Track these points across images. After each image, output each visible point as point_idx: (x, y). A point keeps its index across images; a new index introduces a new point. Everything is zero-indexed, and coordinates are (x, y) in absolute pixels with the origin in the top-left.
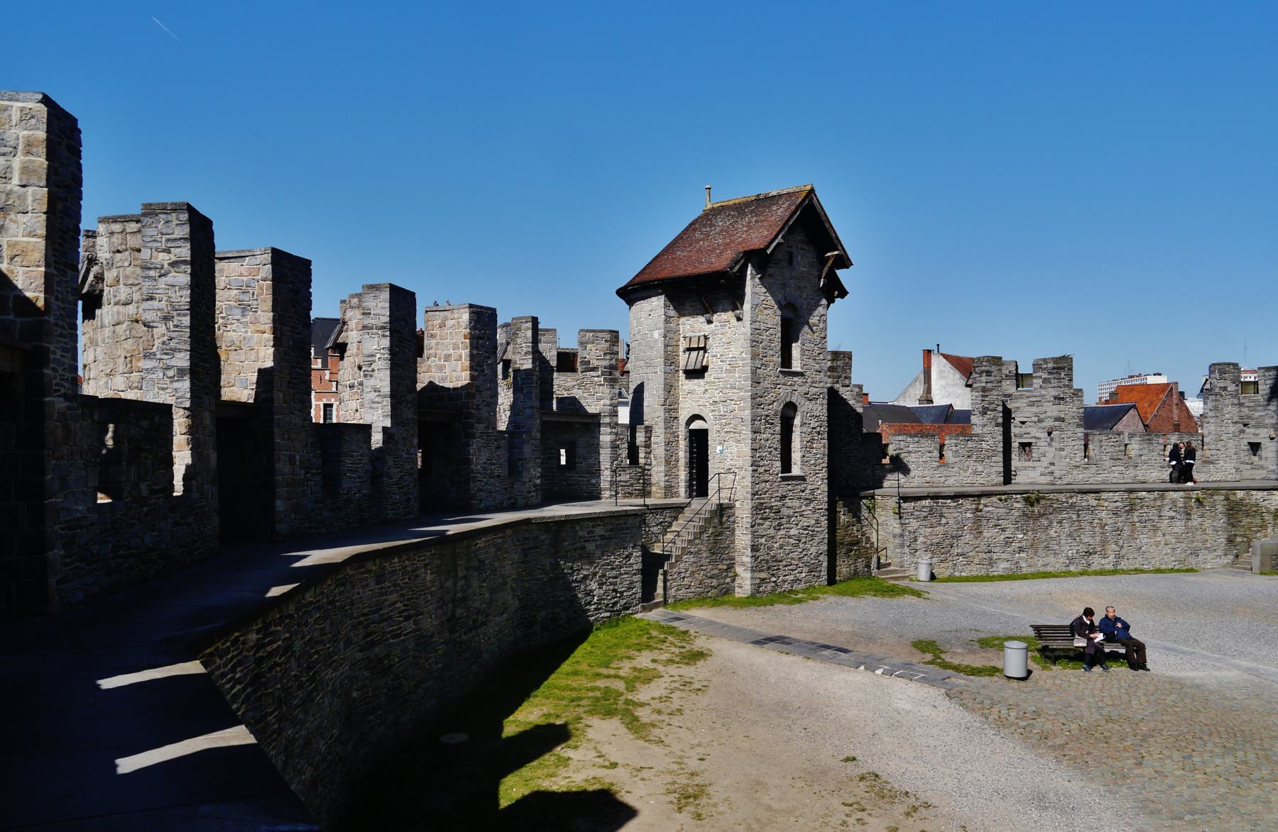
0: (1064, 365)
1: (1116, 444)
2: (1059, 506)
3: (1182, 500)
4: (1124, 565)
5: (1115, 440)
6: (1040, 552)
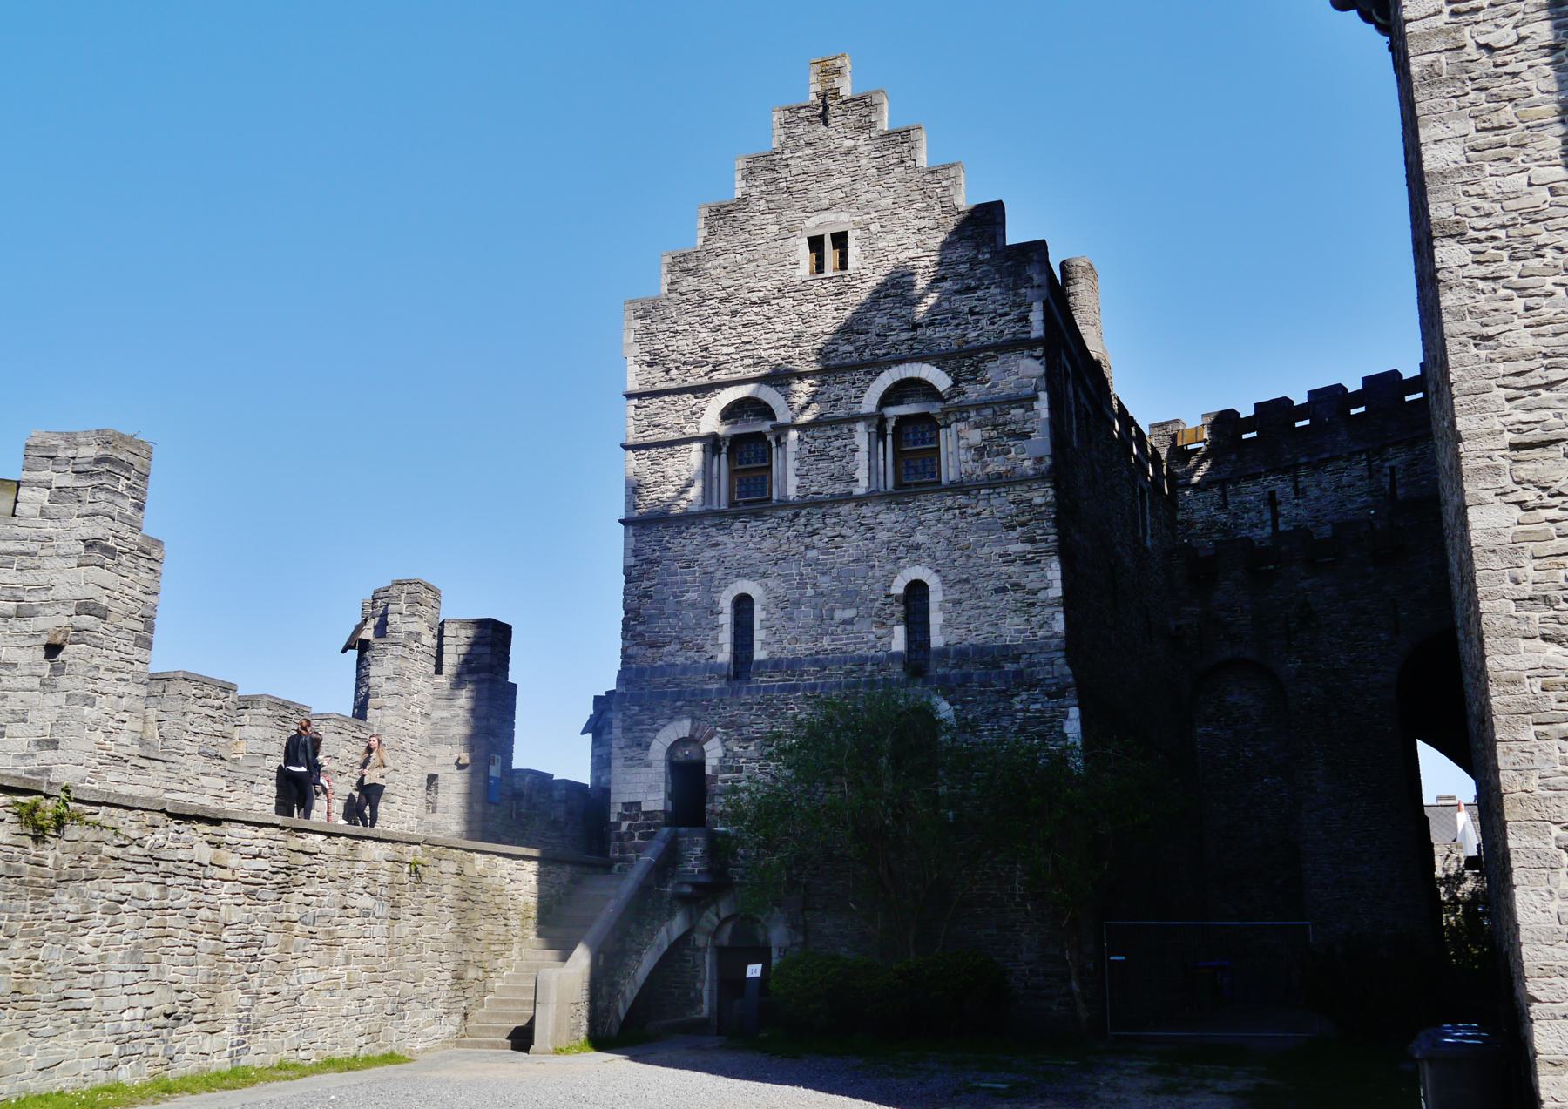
0: (131, 459)
1: (215, 714)
2: (119, 852)
3: (388, 865)
4: (258, 1054)
5: (217, 703)
6: (42, 1019)
